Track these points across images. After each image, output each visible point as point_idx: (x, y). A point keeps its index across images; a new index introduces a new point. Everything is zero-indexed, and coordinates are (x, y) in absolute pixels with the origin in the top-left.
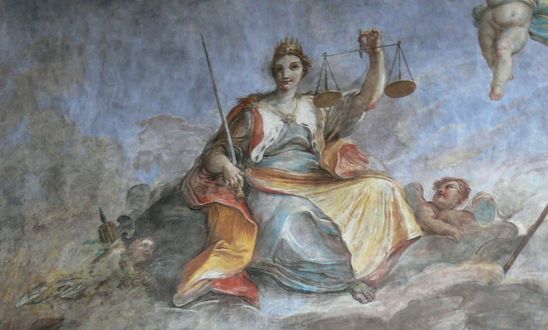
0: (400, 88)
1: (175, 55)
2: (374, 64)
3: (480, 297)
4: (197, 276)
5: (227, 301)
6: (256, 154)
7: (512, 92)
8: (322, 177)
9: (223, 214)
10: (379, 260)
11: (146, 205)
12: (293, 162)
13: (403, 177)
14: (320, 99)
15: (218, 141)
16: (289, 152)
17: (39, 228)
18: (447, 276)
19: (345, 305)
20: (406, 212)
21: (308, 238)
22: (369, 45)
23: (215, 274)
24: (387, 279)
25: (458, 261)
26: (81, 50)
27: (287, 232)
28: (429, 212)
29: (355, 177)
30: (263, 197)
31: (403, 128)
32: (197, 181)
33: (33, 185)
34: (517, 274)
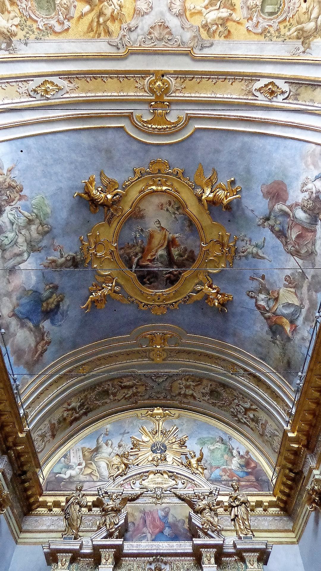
0: (263, 277)
1: (242, 314)
2: (257, 280)
3: (311, 287)
4: (288, 332)
5: (295, 330)
6: (267, 309)
7: (271, 258)
8: (276, 299)
9: (277, 320)
10: (297, 299)
11: (271, 333)
12: (271, 304)
13: (282, 286)
14: (260, 292)
15: (262, 314)
16: (269, 303)
17: (268, 353)
18: (305, 289)
19: (304, 311)
20: (289, 289)
21: (288, 309)
22: (252, 279)
23: (289, 329)
24: (302, 300)
25: (303, 286)
26: (235, 328)
27: (286, 311)
28: (290, 285)
29: (278, 294)
30: (277, 312)
31: (271, 280)
32: (269, 322)
33: (259, 349)
34: (309, 278)
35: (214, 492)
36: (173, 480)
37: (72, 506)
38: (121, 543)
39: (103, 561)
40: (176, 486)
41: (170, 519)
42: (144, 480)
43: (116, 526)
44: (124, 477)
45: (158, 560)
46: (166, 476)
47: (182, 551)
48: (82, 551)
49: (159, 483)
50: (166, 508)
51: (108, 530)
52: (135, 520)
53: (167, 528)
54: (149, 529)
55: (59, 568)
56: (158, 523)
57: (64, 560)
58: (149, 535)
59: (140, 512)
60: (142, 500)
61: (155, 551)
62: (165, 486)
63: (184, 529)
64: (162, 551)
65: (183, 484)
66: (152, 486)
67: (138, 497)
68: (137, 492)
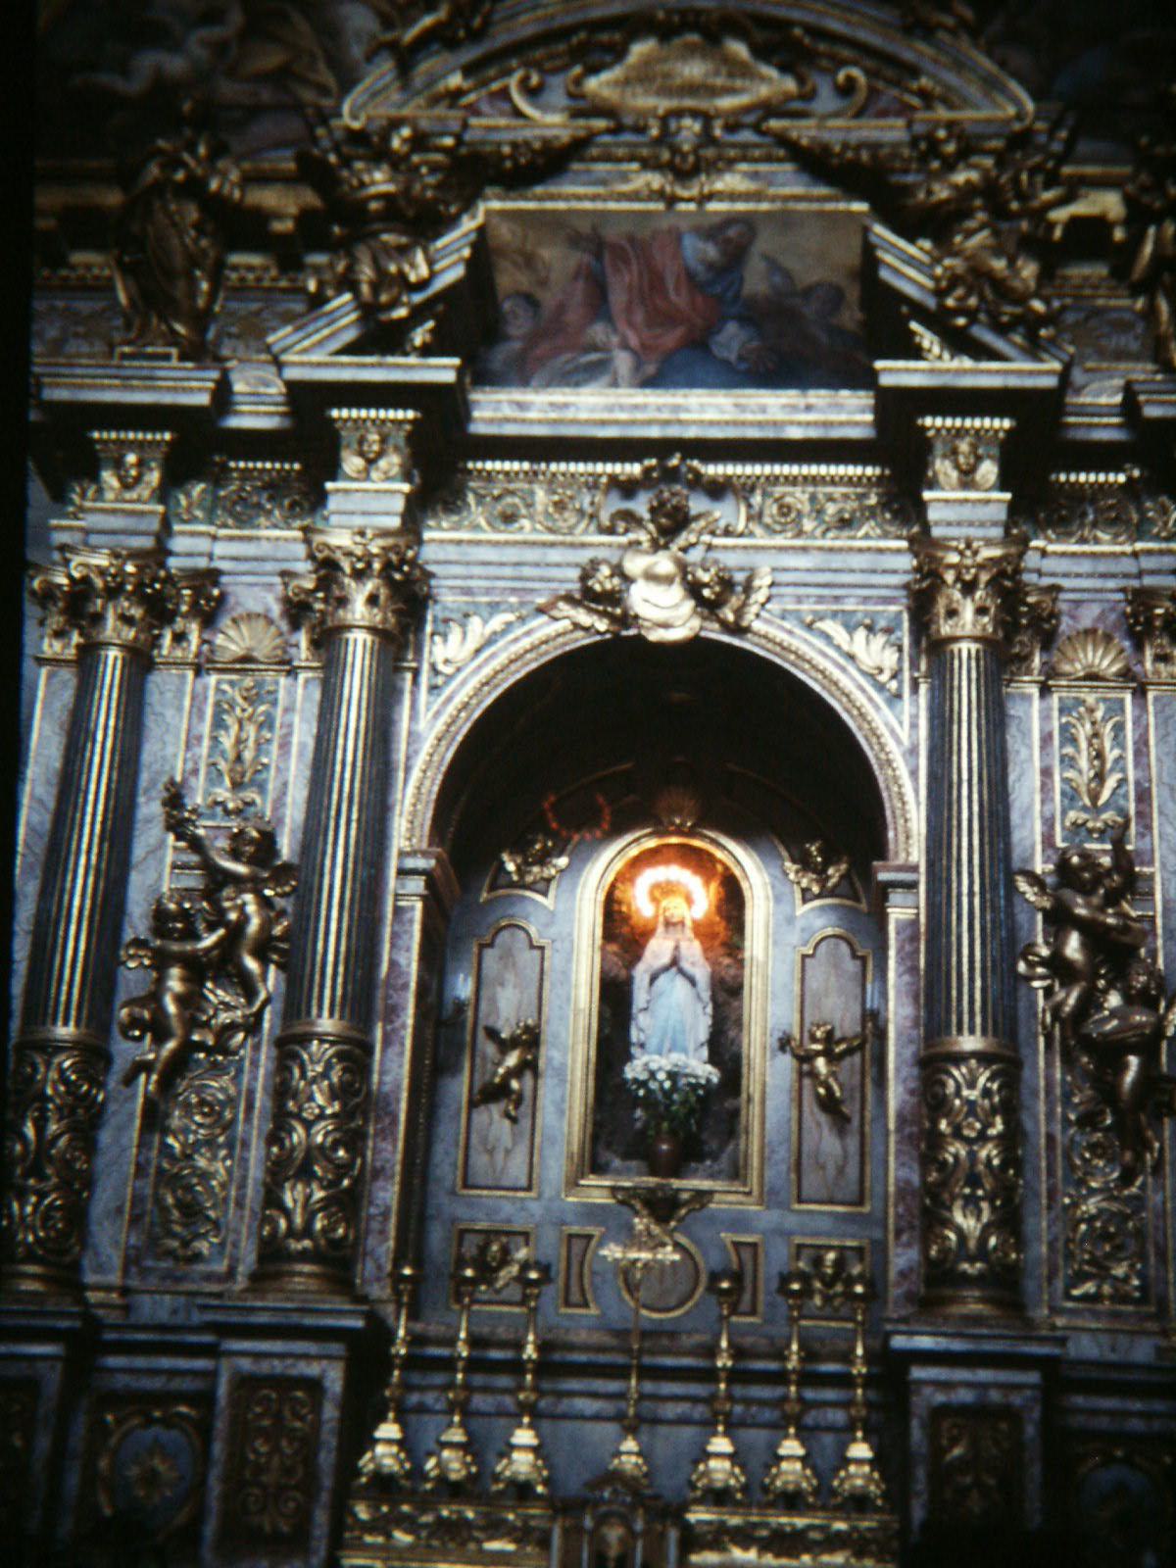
35: (1042, 139)
36: (784, 68)
37: (157, 204)
38: (449, 377)
39: (352, 463)
40: (796, 105)
41: (756, 280)
42: (594, 70)
43: (418, 298)
44: (470, 54)
45: (671, 476)
46: (739, 49)
47: (814, 433)
48: (234, 422)
49: (692, 89)
50: (731, 219)
51: (368, 311)
52: (543, 283)
53: (732, 328)
54: (622, 326)
55: (110, 495)
56: (679, 298)
57: (131, 458)
58: (623, 361)
59: (575, 240)
60: (585, 178)
61: (654, 432)
62: (726, 103)
63: (837, 332)
64: (691, 433)
65: (847, 89)
66: (647, 101)
67: (549, 163)
68: (548, 133)
